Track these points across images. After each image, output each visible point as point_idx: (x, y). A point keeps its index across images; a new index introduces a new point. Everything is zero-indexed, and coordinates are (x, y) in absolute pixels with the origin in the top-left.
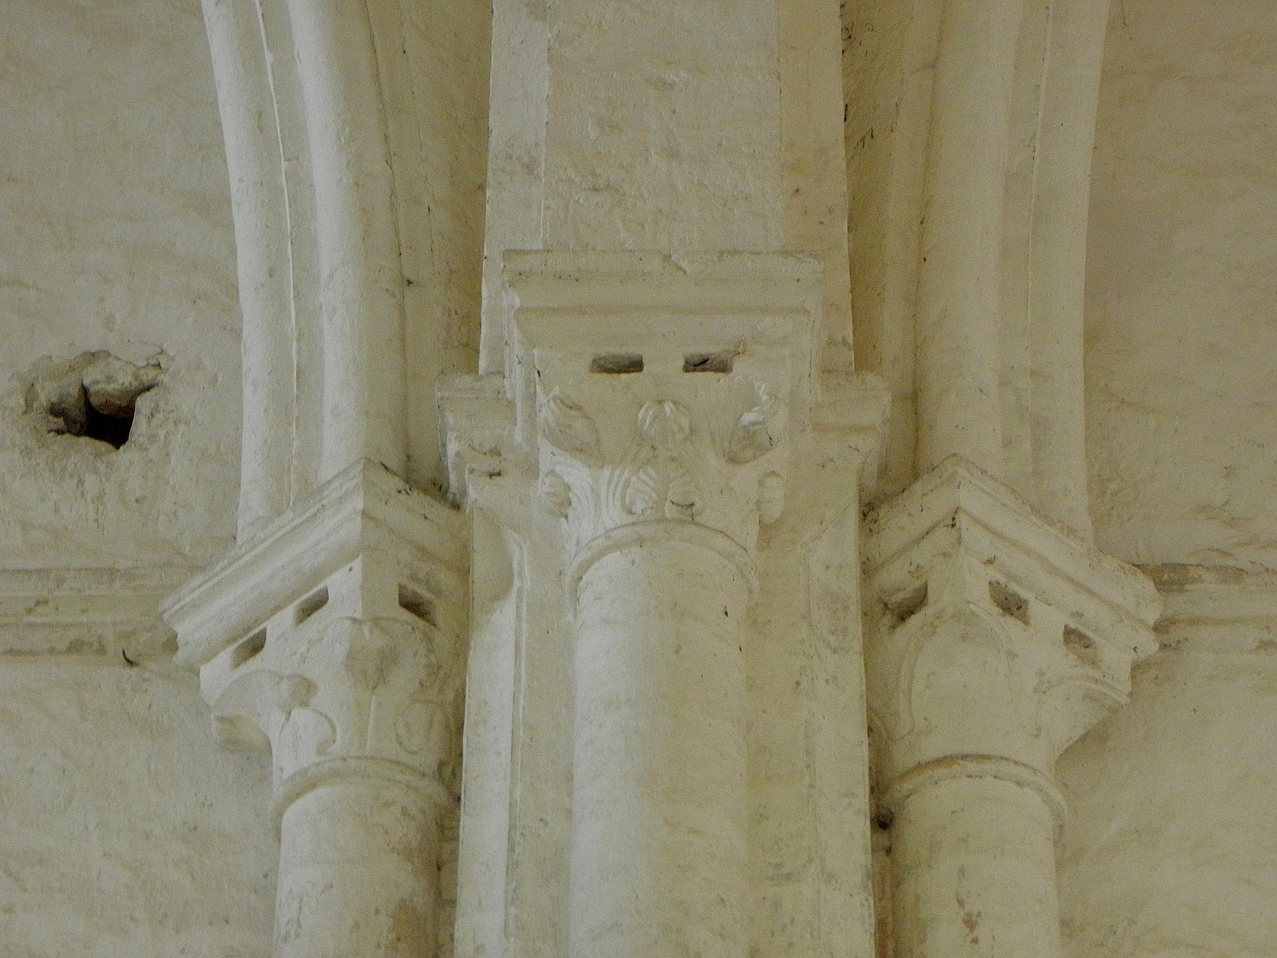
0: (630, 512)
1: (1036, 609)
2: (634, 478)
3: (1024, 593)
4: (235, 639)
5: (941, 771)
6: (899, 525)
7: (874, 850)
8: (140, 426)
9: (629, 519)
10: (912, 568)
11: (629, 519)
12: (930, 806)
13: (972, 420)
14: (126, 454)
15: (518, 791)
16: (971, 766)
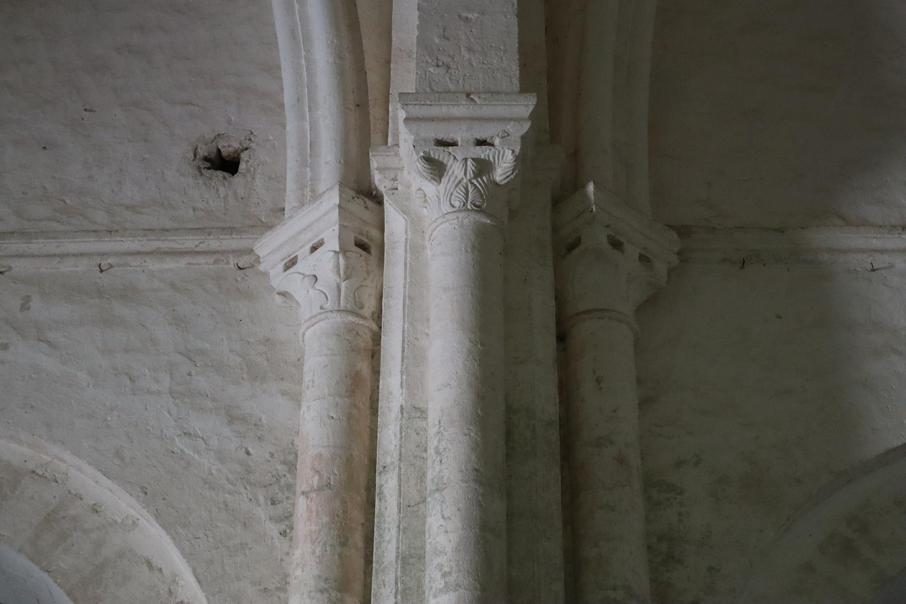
0: (453, 206)
3: (622, 240)
7: (557, 350)
8: (242, 166)
11: (451, 209)
14: (237, 179)
15: (406, 326)
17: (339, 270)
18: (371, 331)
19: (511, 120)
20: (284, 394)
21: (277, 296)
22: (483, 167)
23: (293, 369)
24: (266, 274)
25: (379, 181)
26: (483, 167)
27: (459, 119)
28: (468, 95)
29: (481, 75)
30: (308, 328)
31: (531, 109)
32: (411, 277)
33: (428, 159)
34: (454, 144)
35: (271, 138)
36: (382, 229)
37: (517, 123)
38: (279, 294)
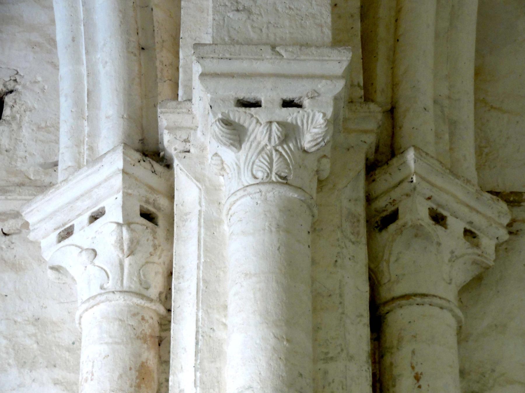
0: (255, 178)
1: (451, 220)
2: (257, 160)
3: (445, 213)
4: (58, 228)
5: (403, 302)
6: (384, 180)
7: (371, 339)
9: (254, 181)
10: (391, 201)
11: (254, 181)
12: (399, 319)
13: (420, 124)
15: (200, 314)
16: (419, 300)
17: (122, 244)
18: (158, 314)
19: (322, 77)
20: (56, 383)
21: (49, 271)
22: (289, 133)
23: (67, 353)
24: (36, 244)
25: (170, 142)
26: (289, 133)
28: (273, 48)
29: (287, 23)
30: (86, 310)
31: (345, 65)
32: (206, 256)
33: (227, 123)
34: (257, 104)
35: (39, 79)
36: (171, 197)
37: (329, 82)
38: (52, 268)
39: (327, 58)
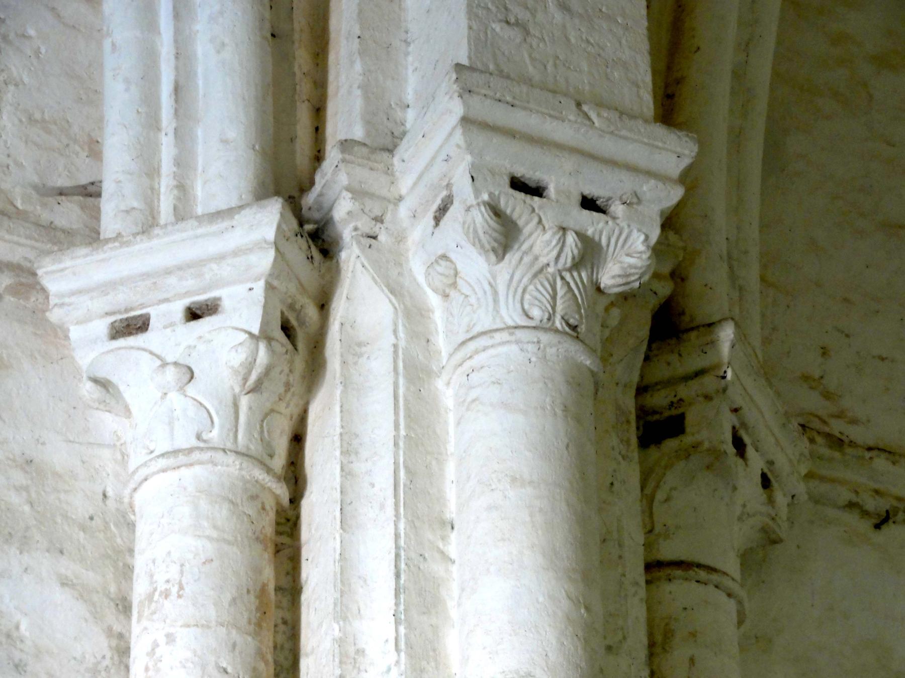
2: (531, 287)
4: (120, 312)
5: (679, 572)
9: (523, 322)
10: (675, 400)
11: (523, 322)
16: (703, 575)
17: (249, 372)
18: (278, 503)
19: (650, 174)
20: (65, 583)
21: (89, 385)
22: (590, 253)
23: (82, 534)
24: (59, 333)
26: (590, 253)
27: (560, 147)
28: (579, 105)
29: (585, 66)
30: (164, 471)
31: (686, 162)
32: (408, 427)
33: (496, 212)
34: (537, 191)
35: (32, 32)
36: (324, 306)
37: (660, 185)
38: (96, 381)
39: (660, 144)
